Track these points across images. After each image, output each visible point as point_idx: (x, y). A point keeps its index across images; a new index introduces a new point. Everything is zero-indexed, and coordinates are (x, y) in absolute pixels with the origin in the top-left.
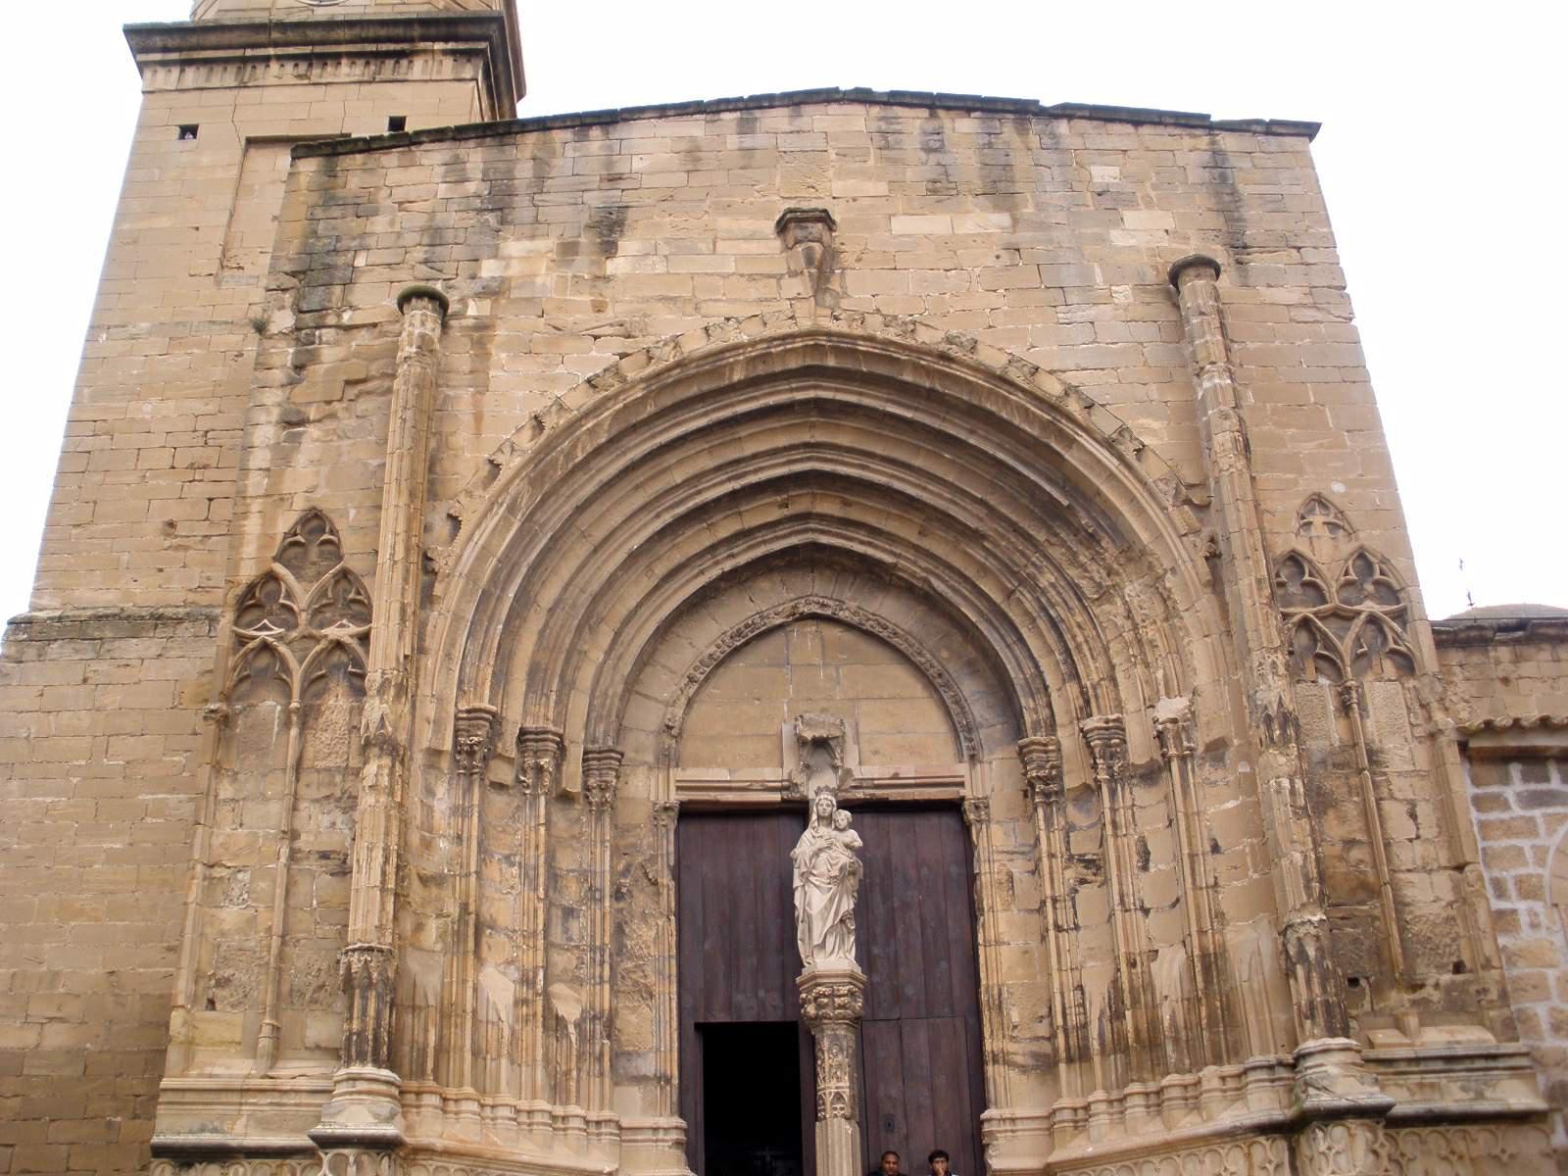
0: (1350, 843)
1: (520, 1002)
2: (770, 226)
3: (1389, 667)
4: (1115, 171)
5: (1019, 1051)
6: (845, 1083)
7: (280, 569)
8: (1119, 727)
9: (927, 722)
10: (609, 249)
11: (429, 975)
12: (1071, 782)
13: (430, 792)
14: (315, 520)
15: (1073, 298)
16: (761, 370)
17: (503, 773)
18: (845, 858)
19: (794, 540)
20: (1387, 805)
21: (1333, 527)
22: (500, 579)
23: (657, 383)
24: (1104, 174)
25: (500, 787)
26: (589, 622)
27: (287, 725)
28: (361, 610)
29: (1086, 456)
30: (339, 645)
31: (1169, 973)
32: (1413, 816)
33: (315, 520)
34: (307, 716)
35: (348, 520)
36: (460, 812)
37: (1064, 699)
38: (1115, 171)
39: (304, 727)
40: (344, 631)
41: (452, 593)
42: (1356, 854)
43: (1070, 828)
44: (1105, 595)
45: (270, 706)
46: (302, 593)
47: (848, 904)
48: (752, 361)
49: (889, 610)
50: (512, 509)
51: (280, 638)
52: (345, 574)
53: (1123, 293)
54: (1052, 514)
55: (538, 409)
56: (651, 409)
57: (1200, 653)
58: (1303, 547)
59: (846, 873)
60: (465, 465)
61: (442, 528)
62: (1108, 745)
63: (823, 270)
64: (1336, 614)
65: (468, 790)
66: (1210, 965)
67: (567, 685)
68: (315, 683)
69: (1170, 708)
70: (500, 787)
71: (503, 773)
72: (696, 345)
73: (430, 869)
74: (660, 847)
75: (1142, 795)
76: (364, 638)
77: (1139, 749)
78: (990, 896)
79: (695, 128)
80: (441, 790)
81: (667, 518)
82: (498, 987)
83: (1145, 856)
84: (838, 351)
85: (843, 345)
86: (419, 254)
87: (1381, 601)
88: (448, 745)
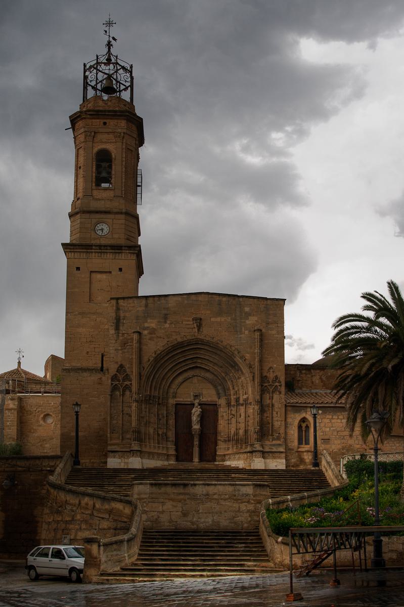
0: (267, 417)
1: (154, 432)
2: (191, 319)
3: (278, 393)
4: (249, 309)
5: (222, 439)
6: (198, 443)
7: (117, 373)
8: (239, 397)
9: (213, 392)
10: (165, 322)
11: (143, 430)
12: (232, 404)
13: (141, 405)
14: (121, 366)
15: (239, 333)
16: (189, 343)
17: (151, 402)
18: (198, 413)
19: (194, 365)
20: (274, 412)
21: (273, 372)
22: (150, 376)
23: (173, 346)
24: (247, 309)
25: (151, 404)
26: (163, 379)
27: (120, 396)
28: (131, 380)
29: (238, 359)
30: (127, 385)
31: (241, 432)
32: (277, 414)
33: (121, 366)
34: (123, 395)
35: (127, 366)
36: (146, 408)
37: (232, 392)
38: (249, 309)
39: (123, 396)
40: (128, 383)
41: (144, 378)
42: (268, 418)
43: (231, 410)
44: (239, 378)
45: (118, 393)
46: (121, 377)
47: (199, 419)
48: (188, 342)
49: (208, 375)
50: (152, 365)
51: (119, 384)
52: (127, 374)
53: (247, 332)
54: (232, 367)
55: (156, 350)
56: (172, 350)
57: (250, 389)
58: (268, 375)
59: (199, 414)
60: (145, 359)
61: (142, 369)
62: (237, 400)
63: (199, 327)
64: (270, 385)
65: (147, 405)
66: (246, 431)
67: (160, 388)
68: (124, 391)
69: (245, 397)
70: (151, 404)
71: (151, 402)
72: (180, 340)
73: (142, 416)
74: (172, 410)
75: (241, 407)
76: (131, 384)
77: (241, 401)
78: (220, 418)
79: (179, 299)
80: (143, 405)
81: (174, 364)
82: (151, 431)
83: (240, 416)
84: (201, 341)
85: (202, 340)
86: (134, 321)
87: (279, 383)
88: (144, 399)
